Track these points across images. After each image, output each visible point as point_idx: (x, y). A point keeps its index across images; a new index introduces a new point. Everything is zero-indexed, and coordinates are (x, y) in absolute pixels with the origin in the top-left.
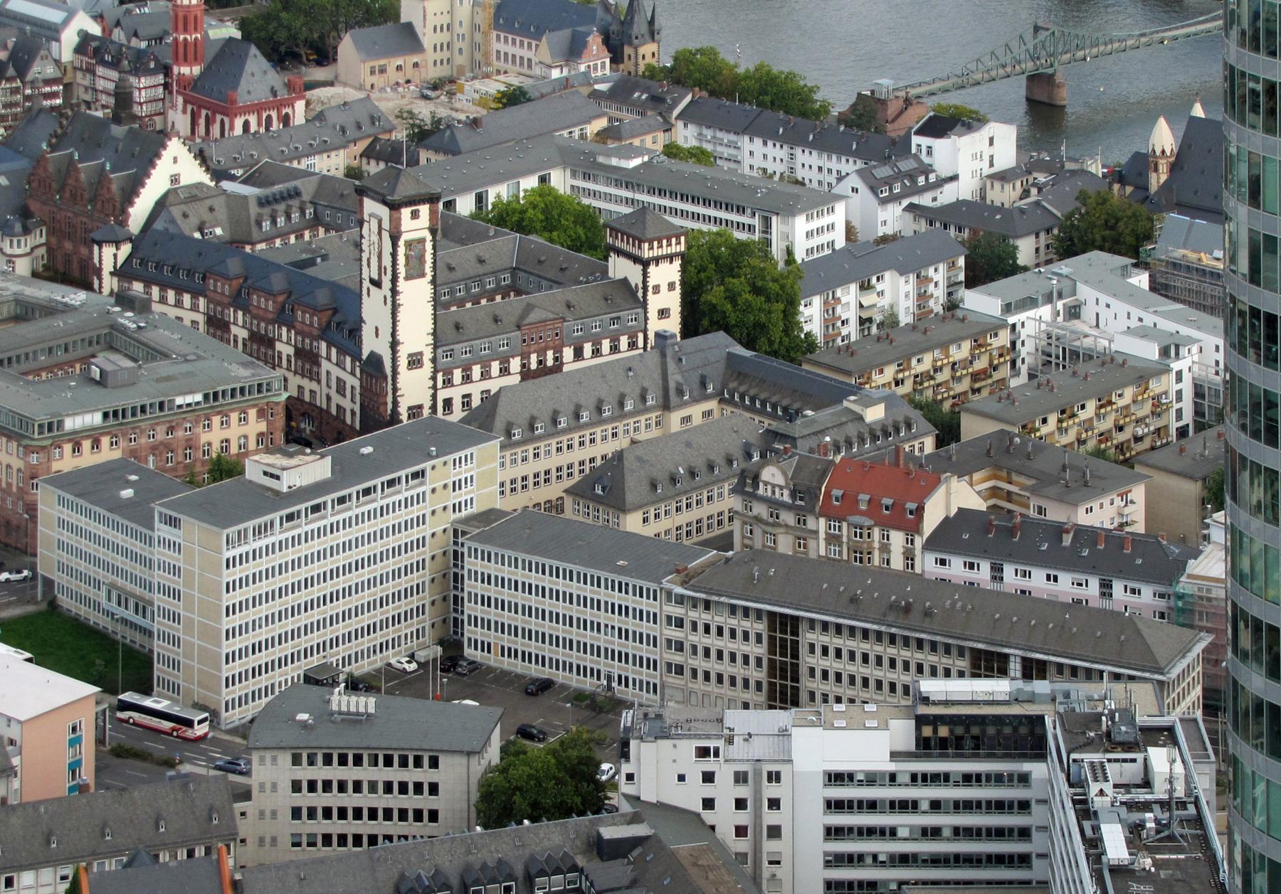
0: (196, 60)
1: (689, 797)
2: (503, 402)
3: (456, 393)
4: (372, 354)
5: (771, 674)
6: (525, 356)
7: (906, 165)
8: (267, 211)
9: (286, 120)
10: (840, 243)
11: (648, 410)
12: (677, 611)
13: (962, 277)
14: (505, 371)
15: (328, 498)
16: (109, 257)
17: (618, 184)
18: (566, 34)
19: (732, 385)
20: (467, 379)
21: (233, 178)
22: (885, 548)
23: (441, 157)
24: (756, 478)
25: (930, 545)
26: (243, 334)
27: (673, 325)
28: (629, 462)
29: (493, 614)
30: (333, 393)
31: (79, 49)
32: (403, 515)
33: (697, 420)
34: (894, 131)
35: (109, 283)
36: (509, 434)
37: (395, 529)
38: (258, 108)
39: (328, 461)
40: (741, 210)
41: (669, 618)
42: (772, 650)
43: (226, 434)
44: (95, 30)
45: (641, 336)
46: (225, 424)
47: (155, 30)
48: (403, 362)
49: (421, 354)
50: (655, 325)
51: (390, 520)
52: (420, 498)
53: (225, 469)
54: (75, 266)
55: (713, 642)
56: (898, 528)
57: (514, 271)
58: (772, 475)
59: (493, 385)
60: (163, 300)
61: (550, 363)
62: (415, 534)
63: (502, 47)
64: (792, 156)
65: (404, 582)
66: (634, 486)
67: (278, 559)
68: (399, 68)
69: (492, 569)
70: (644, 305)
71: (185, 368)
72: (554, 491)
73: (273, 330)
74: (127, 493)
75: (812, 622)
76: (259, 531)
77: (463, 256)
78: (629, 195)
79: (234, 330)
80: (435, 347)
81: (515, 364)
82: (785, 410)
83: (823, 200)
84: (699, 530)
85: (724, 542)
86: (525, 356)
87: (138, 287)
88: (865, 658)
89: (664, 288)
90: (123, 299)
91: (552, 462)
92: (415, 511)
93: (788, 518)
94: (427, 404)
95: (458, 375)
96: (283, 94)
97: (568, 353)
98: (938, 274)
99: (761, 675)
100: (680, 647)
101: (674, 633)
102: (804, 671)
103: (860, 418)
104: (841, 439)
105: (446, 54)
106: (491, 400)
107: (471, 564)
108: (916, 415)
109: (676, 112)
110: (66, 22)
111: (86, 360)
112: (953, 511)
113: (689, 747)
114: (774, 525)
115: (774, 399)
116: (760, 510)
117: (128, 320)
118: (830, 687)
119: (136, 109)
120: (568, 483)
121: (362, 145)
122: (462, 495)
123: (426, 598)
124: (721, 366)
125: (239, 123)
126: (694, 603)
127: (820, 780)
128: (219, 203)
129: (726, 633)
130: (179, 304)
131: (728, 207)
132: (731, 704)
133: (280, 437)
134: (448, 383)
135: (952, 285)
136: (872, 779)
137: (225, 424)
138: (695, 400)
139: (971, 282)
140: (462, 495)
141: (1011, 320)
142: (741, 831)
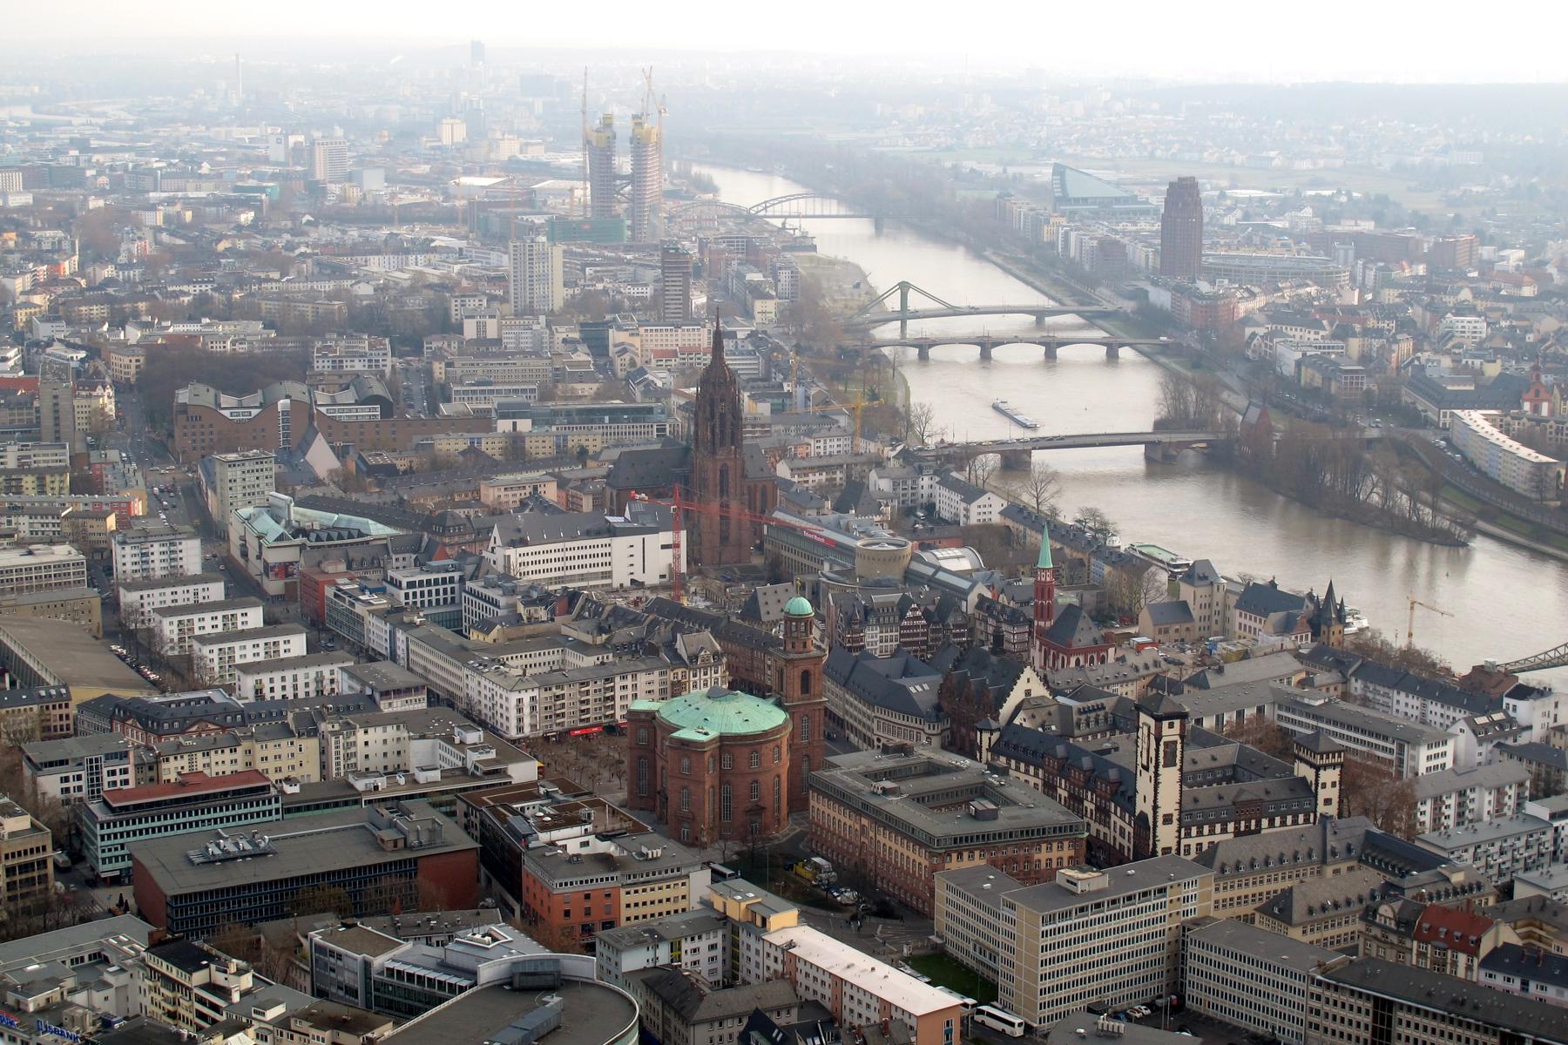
0: (1049, 618)
2: (1220, 850)
3: (1193, 842)
4: (1142, 812)
5: (1374, 1035)
6: (1237, 823)
7: (1497, 717)
8: (1083, 717)
10: (1449, 765)
11: (1312, 863)
12: (1318, 990)
13: (1527, 794)
14: (1224, 831)
15: (1106, 899)
16: (985, 739)
17: (1308, 716)
18: (1281, 614)
19: (1368, 851)
20: (1200, 834)
21: (1065, 695)
22: (1455, 964)
23: (1196, 690)
24: (1375, 912)
25: (1484, 964)
26: (1064, 794)
27: (1332, 810)
29: (1204, 981)
30: (1117, 835)
31: (979, 606)
32: (1152, 915)
35: (986, 756)
36: (1223, 871)
38: (1085, 651)
39: (1107, 877)
40: (1385, 738)
41: (1312, 994)
42: (1375, 1020)
43: (1049, 855)
44: (988, 595)
45: (1312, 815)
46: (1050, 849)
47: (1025, 598)
48: (1160, 820)
49: (1171, 815)
50: (1321, 808)
51: (1144, 917)
52: (1163, 905)
54: (967, 744)
55: (1340, 1012)
56: (1463, 951)
57: (1234, 767)
58: (1385, 910)
60: (1017, 769)
61: (1253, 827)
62: (1158, 927)
63: (1243, 621)
64: (1424, 706)
65: (1151, 956)
66: (1298, 912)
67: (1073, 934)
68: (1177, 630)
71: (1027, 811)
72: (1248, 909)
73: (1083, 793)
75: (1401, 1007)
77: (1203, 757)
78: (1315, 723)
79: (1060, 791)
80: (1181, 812)
81: (1231, 827)
82: (1400, 870)
84: (1338, 942)
85: (1353, 950)
86: (1237, 823)
87: (1003, 760)
88: (1434, 1031)
89: (1329, 785)
90: (993, 769)
91: (1251, 890)
92: (1159, 913)
93: (1394, 939)
94: (1174, 847)
95: (1194, 830)
96: (1101, 643)
97: (1265, 823)
100: (1318, 1013)
101: (1314, 1004)
102: (1394, 1035)
103: (1447, 880)
104: (1434, 892)
105: (1206, 624)
106: (1214, 846)
109: (1350, 672)
110: (972, 588)
111: (967, 803)
112: (1500, 944)
114: (1385, 942)
115: (1394, 862)
116: (1376, 931)
117: (994, 779)
119: (1006, 645)
120: (1258, 904)
121: (1148, 679)
122: (1190, 906)
123: (1164, 967)
124: (1362, 838)
126: (1328, 986)
129: (1347, 1006)
130: (1027, 772)
131: (1378, 736)
133: (1082, 859)
134: (1188, 835)
135: (1519, 796)
137: (1050, 849)
138: (1345, 860)
139: (1533, 798)
140: (1190, 906)
141: (1556, 824)
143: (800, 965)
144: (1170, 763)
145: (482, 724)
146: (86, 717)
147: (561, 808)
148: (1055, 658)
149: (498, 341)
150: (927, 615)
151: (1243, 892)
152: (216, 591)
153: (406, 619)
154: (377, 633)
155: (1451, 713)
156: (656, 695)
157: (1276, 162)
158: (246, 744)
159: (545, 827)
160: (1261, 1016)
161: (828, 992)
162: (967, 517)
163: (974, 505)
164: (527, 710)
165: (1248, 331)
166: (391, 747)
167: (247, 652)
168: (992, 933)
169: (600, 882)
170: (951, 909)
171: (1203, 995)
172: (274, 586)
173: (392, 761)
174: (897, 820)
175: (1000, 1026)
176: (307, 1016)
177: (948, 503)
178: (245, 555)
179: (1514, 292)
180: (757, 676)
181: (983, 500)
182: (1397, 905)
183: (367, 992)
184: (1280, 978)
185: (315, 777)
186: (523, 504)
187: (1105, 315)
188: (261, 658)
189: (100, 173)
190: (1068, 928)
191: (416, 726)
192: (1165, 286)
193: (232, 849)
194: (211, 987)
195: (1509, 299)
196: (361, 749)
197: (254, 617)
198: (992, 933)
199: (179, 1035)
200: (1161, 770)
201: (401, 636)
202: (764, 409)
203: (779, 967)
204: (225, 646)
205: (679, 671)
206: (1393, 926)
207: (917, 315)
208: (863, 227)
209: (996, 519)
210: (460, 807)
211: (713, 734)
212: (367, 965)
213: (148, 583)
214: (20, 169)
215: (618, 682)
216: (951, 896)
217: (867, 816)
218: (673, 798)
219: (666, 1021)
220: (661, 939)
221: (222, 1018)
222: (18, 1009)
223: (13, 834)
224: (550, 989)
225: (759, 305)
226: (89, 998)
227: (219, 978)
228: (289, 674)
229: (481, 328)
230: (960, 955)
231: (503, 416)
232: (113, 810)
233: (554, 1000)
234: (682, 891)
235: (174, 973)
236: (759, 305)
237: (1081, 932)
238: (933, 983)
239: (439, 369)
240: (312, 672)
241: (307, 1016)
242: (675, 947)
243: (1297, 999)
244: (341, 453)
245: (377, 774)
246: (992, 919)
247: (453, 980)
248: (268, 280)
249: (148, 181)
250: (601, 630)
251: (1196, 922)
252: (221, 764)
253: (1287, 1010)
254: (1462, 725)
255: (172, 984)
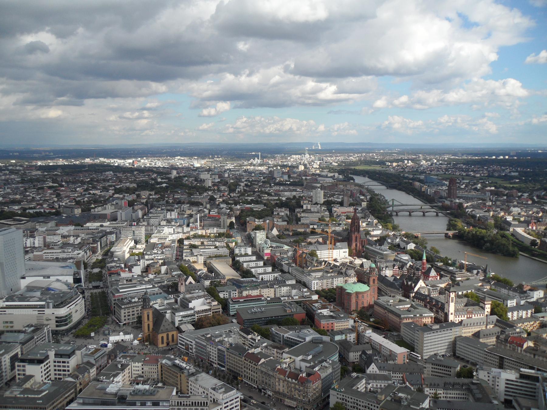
1: (486, 379)
9: (437, 279)
12: (486, 353)
17: (482, 293)
22: (518, 349)
26: (429, 307)
28: (481, 332)
31: (409, 267)
33: (491, 327)
34: (525, 290)
35: (412, 298)
37: (448, 336)
40: (500, 298)
44: (412, 264)
52: (451, 332)
53: (425, 325)
59: (463, 318)
62: (450, 337)
66: (481, 335)
69: (461, 344)
70: (484, 310)
74: (412, 326)
75: (506, 358)
76: (429, 334)
77: (459, 300)
81: (466, 316)
83: (512, 298)
92: (450, 334)
93: (504, 343)
95: (457, 316)
97: (473, 315)
98: (529, 311)
99: (498, 364)
100: (486, 358)
101: (486, 356)
106: (462, 321)
107: (458, 342)
108: (524, 331)
113: (486, 372)
116: (499, 341)
118: (507, 367)
121: (447, 283)
122: (457, 333)
125: (430, 279)
127: (505, 380)
128: (427, 289)
132: (493, 367)
135: (532, 313)
136: (512, 381)
138: (491, 325)
140: (457, 333)
142: (493, 385)
143: (372, 341)
144: (452, 302)
145: (307, 287)
146: (228, 282)
147: (323, 305)
148: (426, 278)
149: (310, 210)
150: (399, 268)
151: (469, 330)
152: (254, 258)
153: (292, 265)
154: (286, 268)
155: (515, 293)
156: (342, 283)
157: (472, 175)
158: (259, 289)
159: (320, 309)
160: (473, 358)
161: (378, 347)
162: (407, 248)
163: (408, 245)
164: (316, 284)
165: (467, 210)
166: (288, 291)
167: (260, 270)
168: (413, 336)
169: (331, 321)
170: (404, 331)
171: (460, 353)
172: (266, 258)
173: (288, 294)
174: (393, 312)
175: (416, 357)
176: (271, 346)
177: (402, 245)
178: (260, 251)
179: (526, 203)
180: (363, 280)
181: (410, 244)
182: (504, 336)
183: (283, 341)
184: (478, 350)
185: (273, 297)
186: (315, 243)
187: (435, 206)
188: (263, 272)
189: (233, 175)
190: (431, 336)
191: (293, 287)
192: (449, 201)
193: (257, 310)
194: (252, 339)
195: (525, 204)
196: (282, 292)
197: (261, 263)
198: (413, 336)
199: (246, 348)
200: (450, 303)
201: (290, 268)
202: (364, 224)
203: (368, 341)
204: (256, 269)
205: (347, 278)
206: (503, 340)
207: (396, 206)
208: (384, 187)
209: (413, 248)
210: (302, 304)
211: (354, 291)
212: (283, 336)
213: (241, 256)
214: (218, 174)
215: (334, 279)
216: (405, 328)
217: (387, 310)
218: (345, 304)
219: (344, 351)
220: (343, 334)
221: (254, 345)
222: (214, 341)
223: (214, 305)
224: (321, 343)
225: (363, 203)
226: (228, 339)
227: (254, 337)
228: (268, 275)
229: (307, 207)
230: (406, 341)
231: (312, 225)
232: (233, 301)
233: (321, 345)
234: (347, 324)
235: (245, 335)
236: (363, 203)
237: (433, 337)
238: (401, 346)
239: (299, 215)
240: (273, 275)
241: (271, 346)
242: (346, 336)
243: (481, 355)
244: (279, 231)
245: (285, 297)
246: (414, 334)
247: (300, 340)
248: (265, 197)
249: (242, 177)
250: (331, 269)
251: (459, 337)
252: (255, 293)
253: (479, 357)
254: (518, 296)
255: (244, 338)
